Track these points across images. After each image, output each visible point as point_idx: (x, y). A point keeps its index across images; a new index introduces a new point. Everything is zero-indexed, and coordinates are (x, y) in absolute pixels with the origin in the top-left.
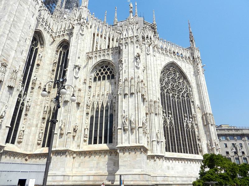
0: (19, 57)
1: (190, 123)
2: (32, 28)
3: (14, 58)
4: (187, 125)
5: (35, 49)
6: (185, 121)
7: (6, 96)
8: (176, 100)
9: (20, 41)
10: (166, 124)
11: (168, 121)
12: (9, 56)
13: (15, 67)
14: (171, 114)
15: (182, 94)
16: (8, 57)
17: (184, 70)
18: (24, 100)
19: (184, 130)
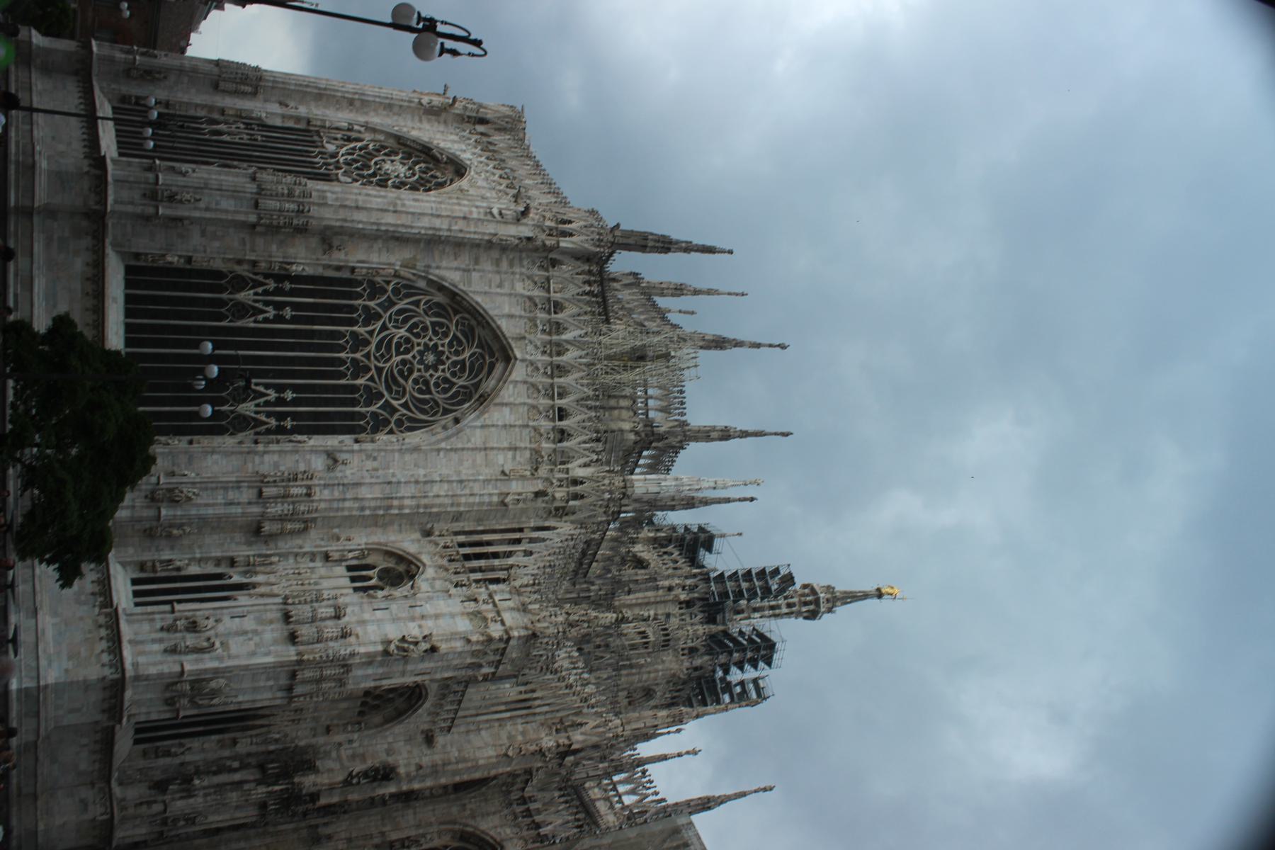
8: (343, 355)
11: (246, 296)
15: (383, 396)
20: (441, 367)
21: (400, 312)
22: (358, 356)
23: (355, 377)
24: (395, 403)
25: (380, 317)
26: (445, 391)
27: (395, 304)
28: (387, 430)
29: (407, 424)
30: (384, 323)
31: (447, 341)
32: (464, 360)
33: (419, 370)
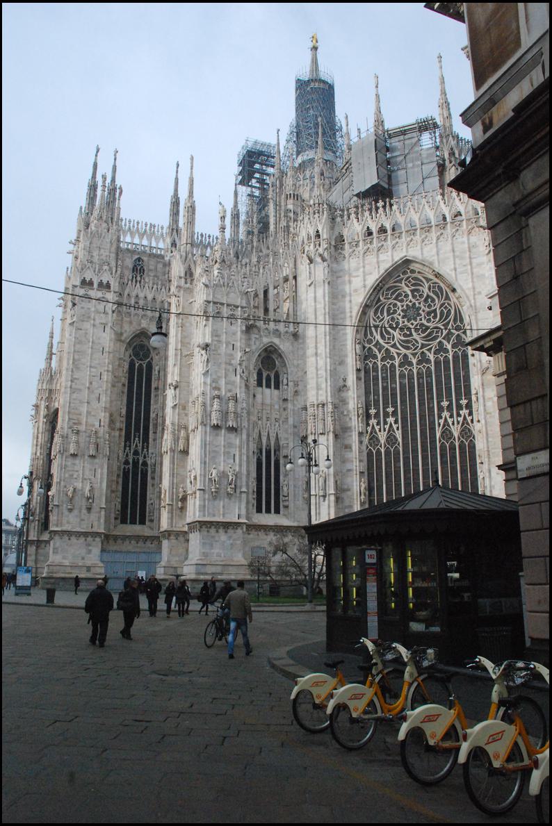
0: (95, 407)
1: (458, 423)
2: (107, 349)
3: (88, 413)
4: (447, 434)
5: (145, 366)
6: (442, 421)
7: (91, 470)
8: (415, 371)
9: (91, 383)
10: (377, 445)
11: (382, 437)
12: (80, 415)
13: (93, 426)
14: (394, 414)
16: (79, 416)
17: (446, 270)
18: (145, 457)
19: (434, 448)
20: (417, 305)
21: (383, 337)
22: (414, 361)
23: (428, 361)
24: (445, 332)
25: (387, 349)
26: (433, 300)
27: (378, 341)
28: (463, 336)
29: (458, 323)
30: (392, 346)
31: (399, 304)
32: (411, 291)
33: (421, 320)
